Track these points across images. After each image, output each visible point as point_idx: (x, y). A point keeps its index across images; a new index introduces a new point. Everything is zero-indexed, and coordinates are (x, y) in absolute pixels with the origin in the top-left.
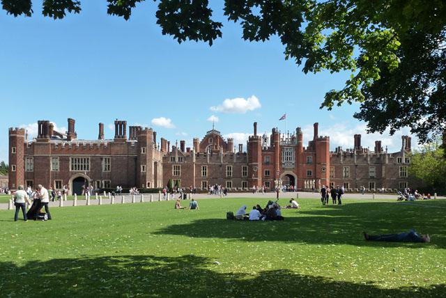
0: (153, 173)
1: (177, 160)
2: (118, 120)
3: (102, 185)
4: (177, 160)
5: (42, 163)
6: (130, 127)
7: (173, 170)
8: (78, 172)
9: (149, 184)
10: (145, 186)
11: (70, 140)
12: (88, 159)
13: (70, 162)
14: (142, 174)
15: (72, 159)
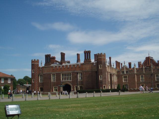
0: (109, 80)
1: (125, 73)
2: (86, 51)
3: (78, 89)
4: (125, 73)
5: (47, 78)
6: (95, 55)
7: (123, 79)
8: (66, 82)
9: (104, 87)
10: (102, 88)
11: (62, 64)
12: (70, 74)
13: (61, 76)
14: (100, 81)
15: (62, 74)
